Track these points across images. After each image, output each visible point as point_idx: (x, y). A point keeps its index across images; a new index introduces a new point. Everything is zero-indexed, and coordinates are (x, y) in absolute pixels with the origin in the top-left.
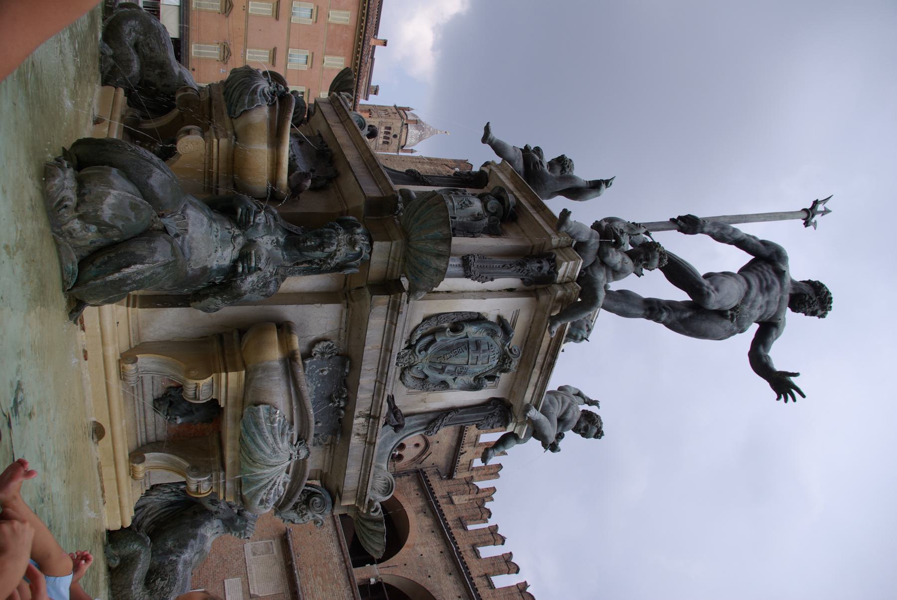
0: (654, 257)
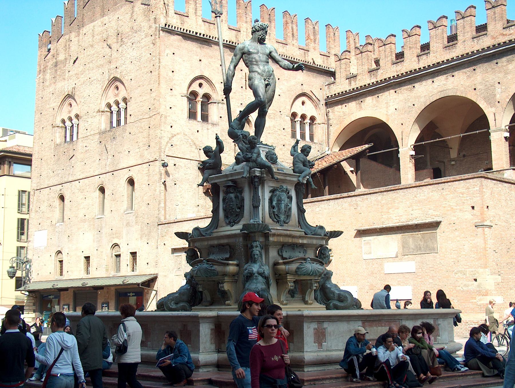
0: (254, 142)
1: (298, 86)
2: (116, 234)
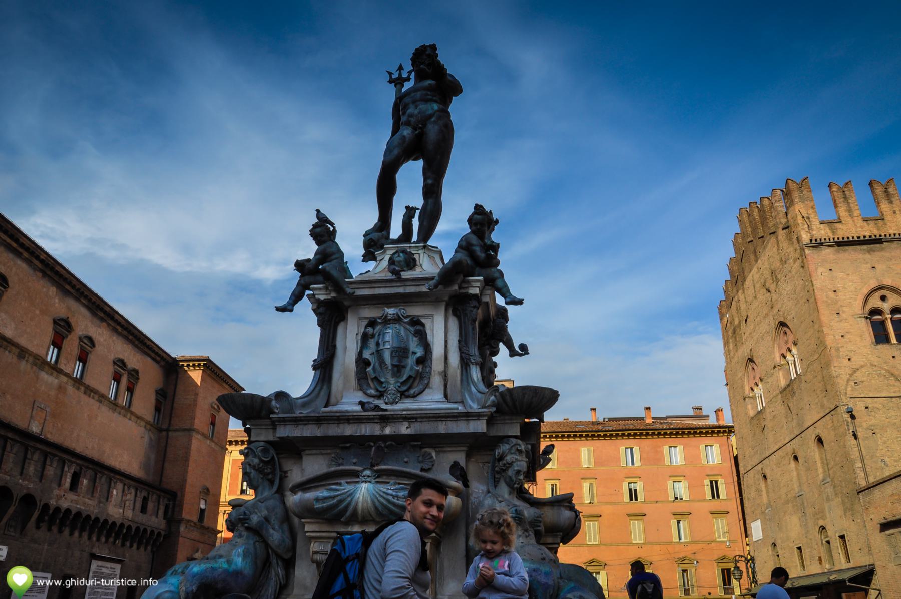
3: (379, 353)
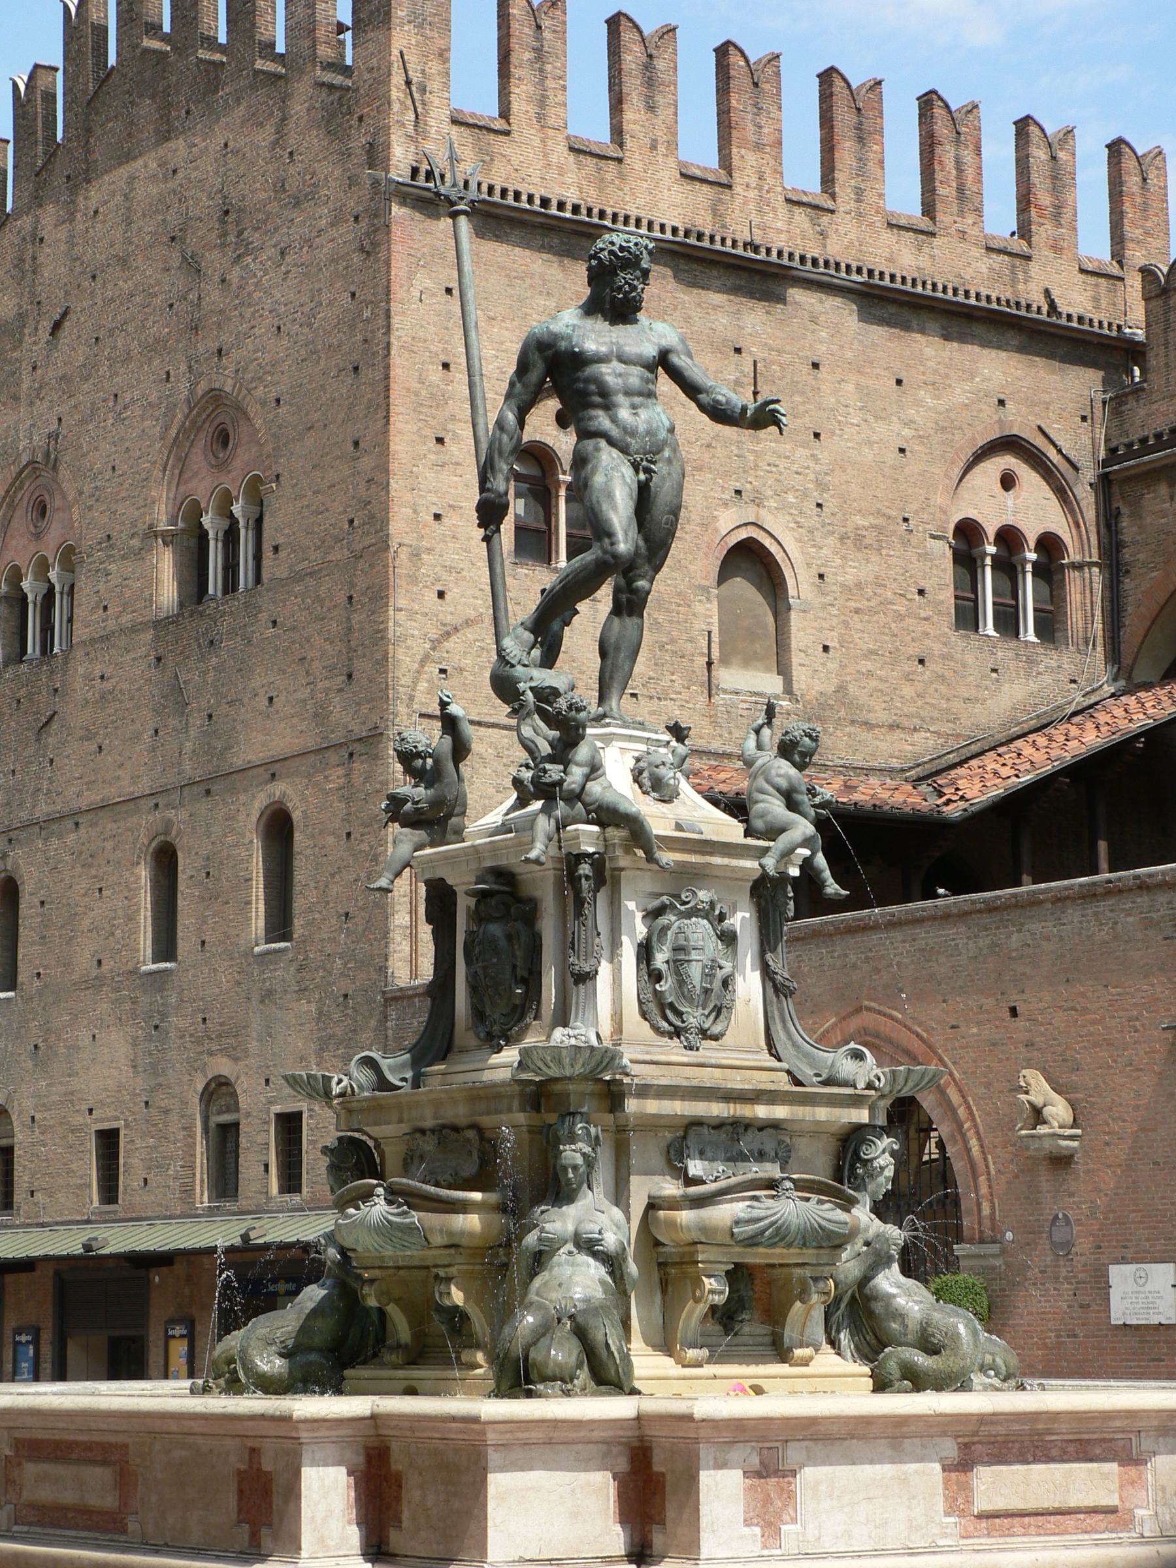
0: (575, 720)
1: (984, 407)
2: (220, 1036)
3: (678, 964)
